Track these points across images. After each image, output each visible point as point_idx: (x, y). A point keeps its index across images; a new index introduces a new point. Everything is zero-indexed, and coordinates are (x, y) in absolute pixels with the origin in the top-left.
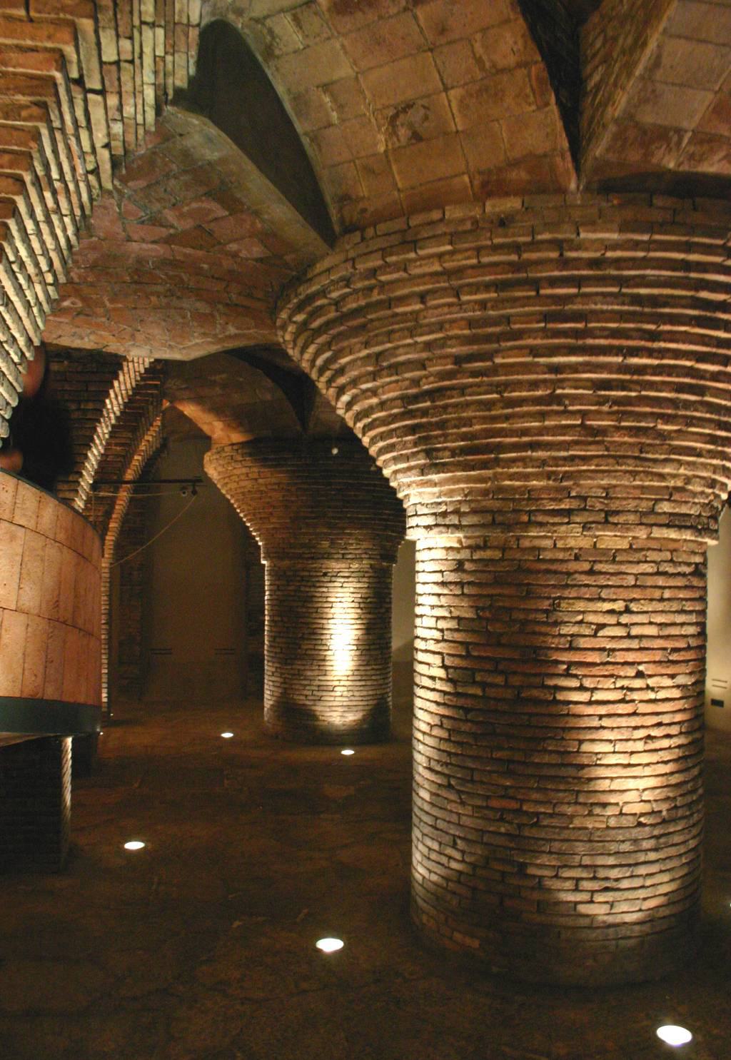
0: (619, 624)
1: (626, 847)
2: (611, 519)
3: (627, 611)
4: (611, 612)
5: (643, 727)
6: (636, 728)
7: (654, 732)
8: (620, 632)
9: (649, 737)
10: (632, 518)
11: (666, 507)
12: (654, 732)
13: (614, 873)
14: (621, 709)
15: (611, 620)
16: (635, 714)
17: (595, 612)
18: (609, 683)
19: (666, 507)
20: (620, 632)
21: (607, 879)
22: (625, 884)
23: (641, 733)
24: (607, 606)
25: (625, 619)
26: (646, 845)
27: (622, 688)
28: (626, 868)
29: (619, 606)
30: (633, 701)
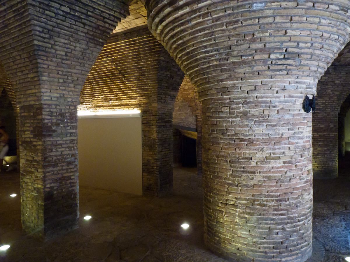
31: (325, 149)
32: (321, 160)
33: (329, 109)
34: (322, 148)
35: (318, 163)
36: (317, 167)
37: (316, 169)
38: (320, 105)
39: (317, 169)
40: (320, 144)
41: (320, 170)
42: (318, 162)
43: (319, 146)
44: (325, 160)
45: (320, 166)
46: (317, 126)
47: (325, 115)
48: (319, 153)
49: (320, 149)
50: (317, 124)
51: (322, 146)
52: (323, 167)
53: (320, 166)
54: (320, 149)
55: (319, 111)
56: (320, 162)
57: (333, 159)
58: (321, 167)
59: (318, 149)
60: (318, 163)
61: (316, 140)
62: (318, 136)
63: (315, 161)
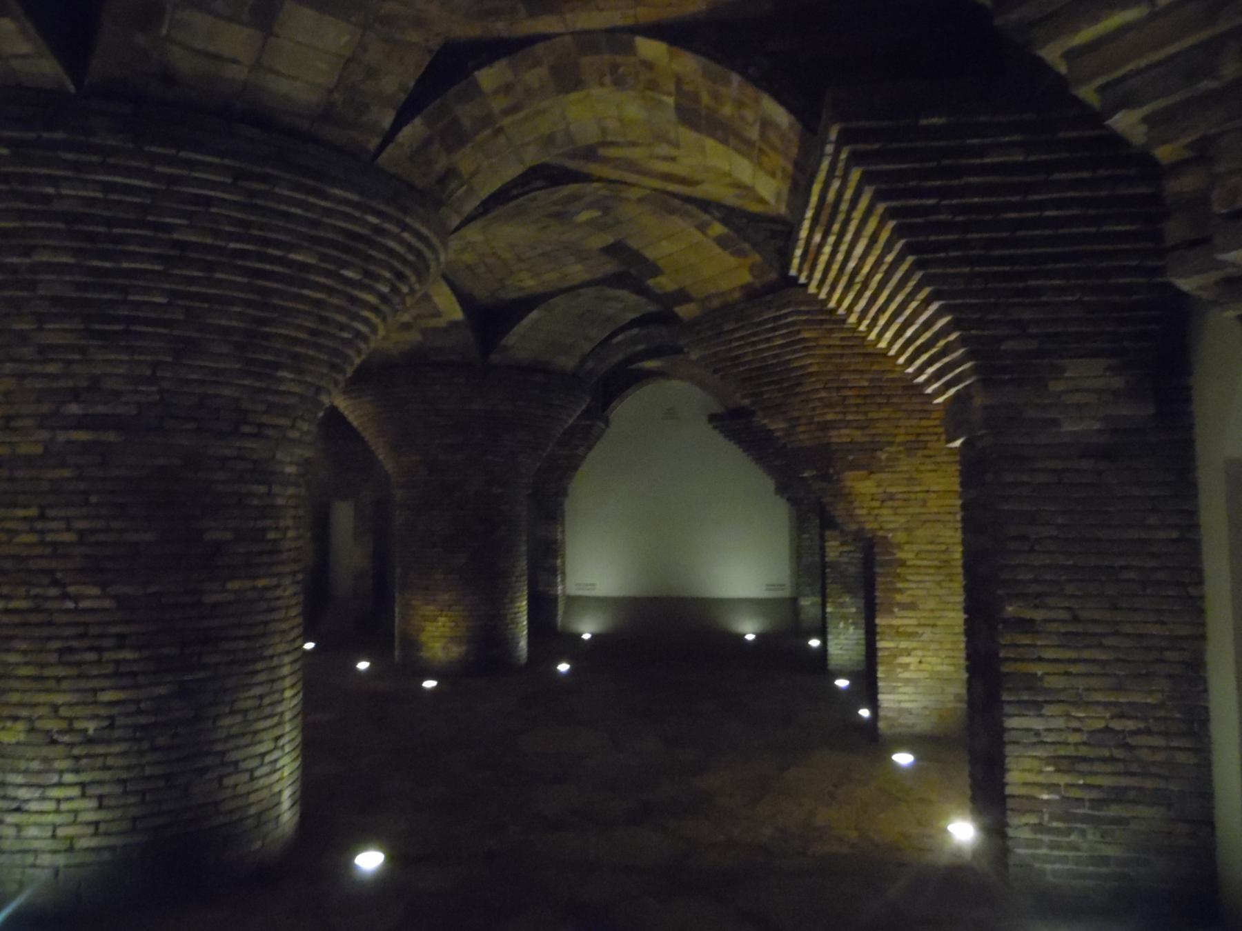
0: (32, 531)
1: (36, 765)
2: (13, 424)
3: (42, 517)
4: (25, 519)
5: (57, 638)
6: (49, 639)
7: (75, 644)
8: (32, 538)
9: (71, 650)
10: (30, 422)
11: (74, 408)
12: (75, 644)
13: (23, 793)
14: (33, 618)
15: (25, 526)
16: (50, 624)
17: (13, 519)
18: (22, 591)
19: (74, 408)
20: (32, 538)
21: (15, 799)
22: (33, 806)
23: (57, 644)
24: (21, 513)
25: (39, 525)
26: (59, 765)
27: (36, 597)
28: (32, 790)
29: (33, 512)
30: (46, 610)
31: (162, 690)
32: (124, 775)
33: (191, 426)
34: (137, 687)
35: (100, 798)
36: (96, 824)
37: (83, 843)
38: (117, 394)
39: (93, 842)
40: (118, 662)
41: (112, 848)
42: (105, 790)
43: (116, 674)
44: (159, 770)
45: (118, 813)
46: (101, 537)
47: (161, 461)
48: (112, 726)
49: (120, 695)
50: (100, 524)
51: (134, 674)
52: (135, 819)
53: (118, 813)
54: (120, 695)
55: (111, 437)
56: (117, 789)
57: (223, 753)
58: (125, 825)
59: (106, 697)
60: (100, 798)
61: (94, 630)
62: (107, 603)
63: (83, 785)
